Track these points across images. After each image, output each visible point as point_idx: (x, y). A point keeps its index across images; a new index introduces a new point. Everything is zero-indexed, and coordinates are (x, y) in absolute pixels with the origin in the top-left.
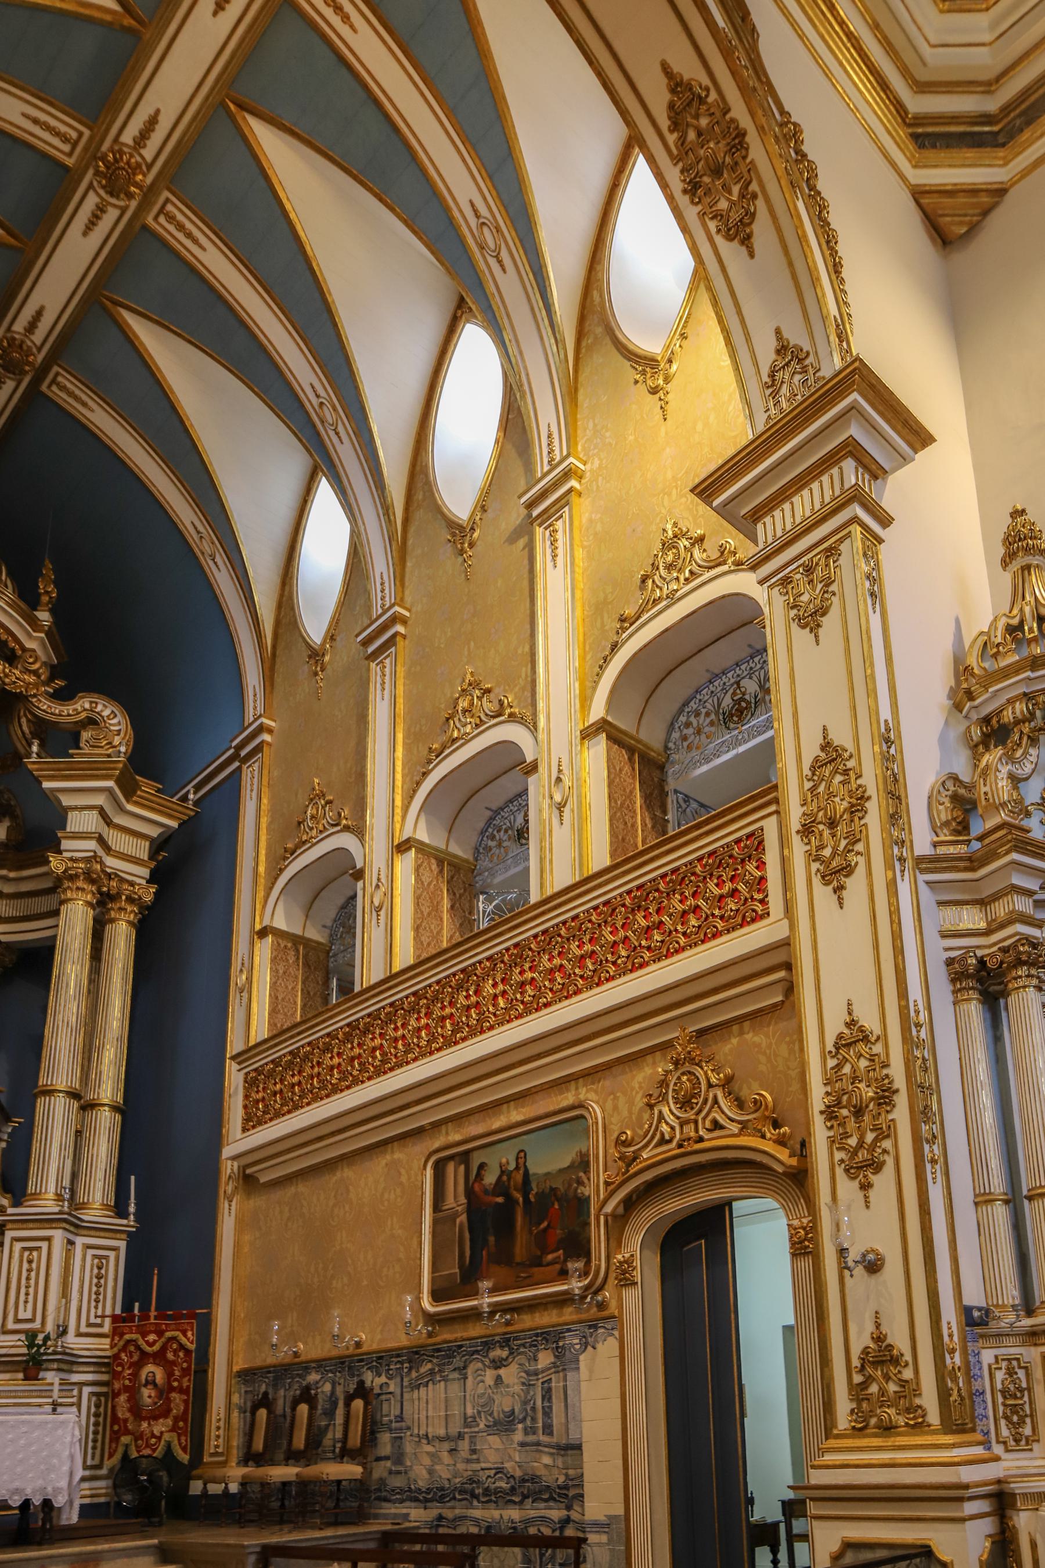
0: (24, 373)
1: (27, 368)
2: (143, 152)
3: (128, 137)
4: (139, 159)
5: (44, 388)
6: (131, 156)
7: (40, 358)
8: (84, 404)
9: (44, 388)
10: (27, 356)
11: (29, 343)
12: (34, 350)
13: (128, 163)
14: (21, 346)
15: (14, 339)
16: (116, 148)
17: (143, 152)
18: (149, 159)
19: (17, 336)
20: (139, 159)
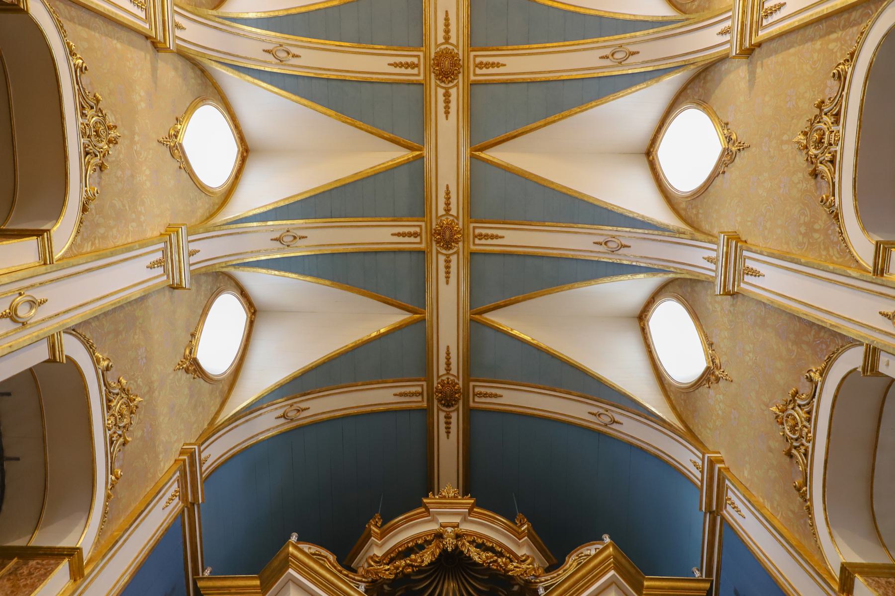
0: (457, 401)
1: (457, 396)
2: (451, 213)
3: (441, 212)
4: (451, 218)
5: (472, 404)
6: (447, 219)
7: (461, 383)
8: (496, 396)
9: (472, 404)
10: (454, 386)
11: (452, 378)
12: (456, 381)
13: (447, 224)
14: (448, 383)
15: (443, 381)
16: (439, 221)
17: (451, 213)
18: (455, 214)
19: (444, 378)
20: (451, 218)
